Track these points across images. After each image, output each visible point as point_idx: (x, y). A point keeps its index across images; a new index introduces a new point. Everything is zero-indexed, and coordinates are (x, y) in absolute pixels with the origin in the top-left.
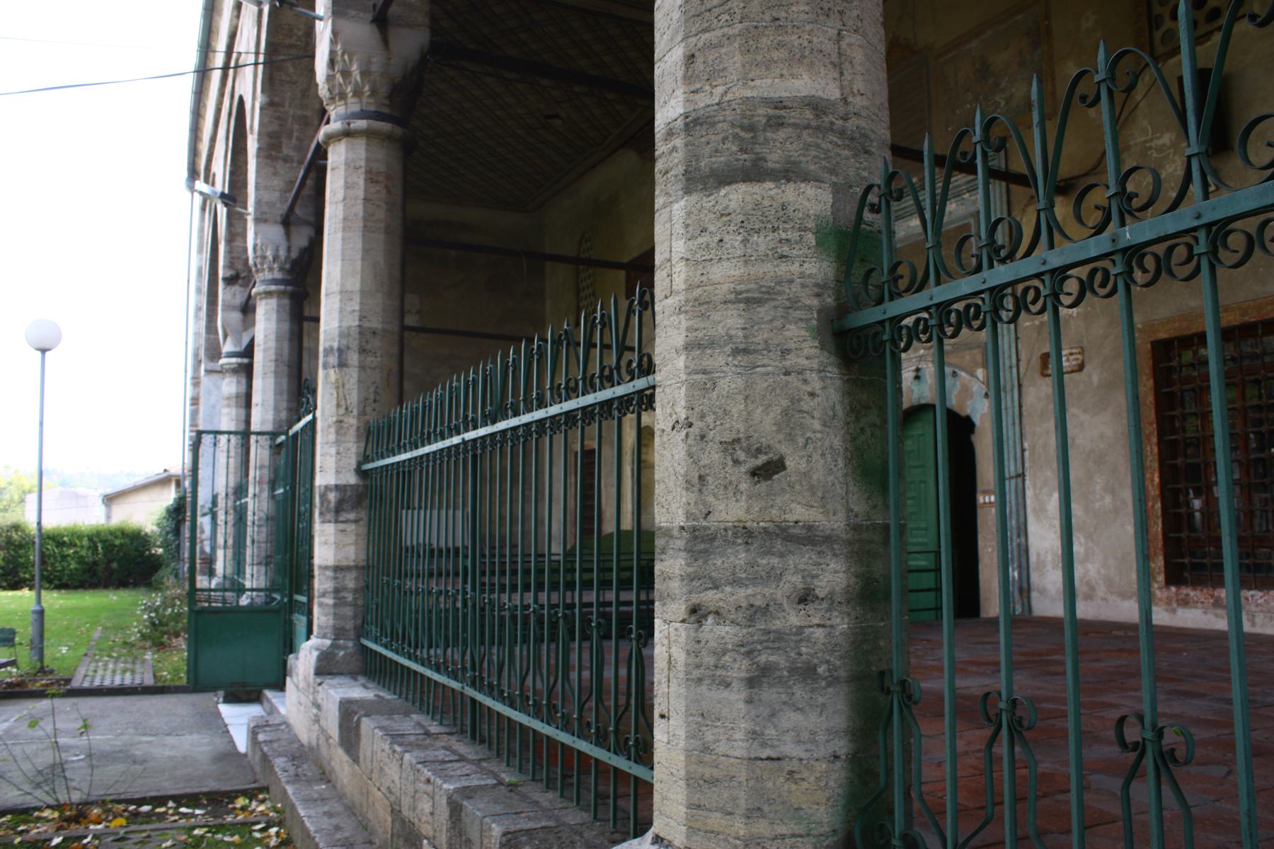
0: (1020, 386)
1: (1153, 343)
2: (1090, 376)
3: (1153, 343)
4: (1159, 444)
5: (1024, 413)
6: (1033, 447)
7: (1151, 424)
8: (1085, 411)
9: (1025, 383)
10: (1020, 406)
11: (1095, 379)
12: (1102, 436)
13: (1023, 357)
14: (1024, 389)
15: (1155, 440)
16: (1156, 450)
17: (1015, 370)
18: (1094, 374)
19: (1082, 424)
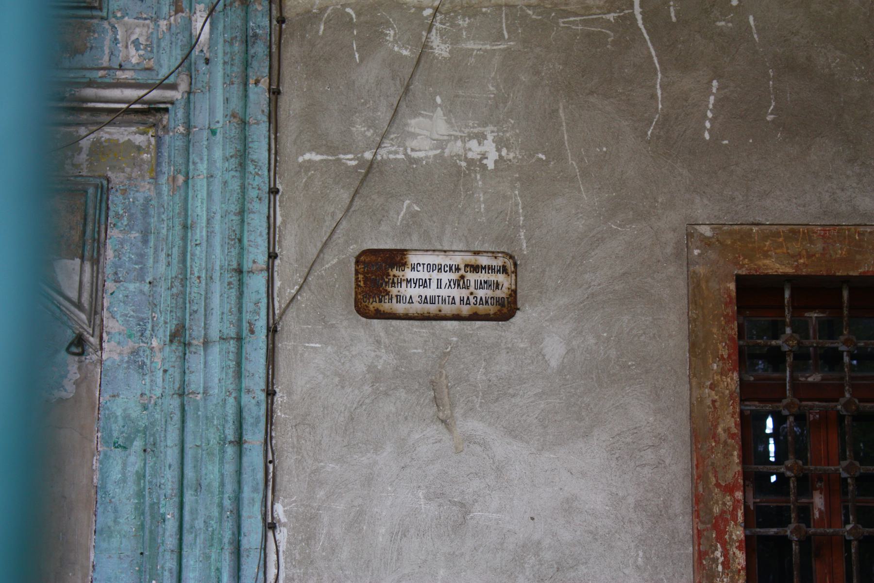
0: (272, 331)
1: (740, 280)
2: (536, 339)
3: (740, 280)
4: (750, 545)
5: (279, 414)
6: (307, 524)
7: (729, 489)
8: (512, 433)
9: (290, 325)
10: (270, 393)
11: (555, 349)
12: (569, 507)
13: (288, 248)
14: (284, 345)
15: (738, 533)
16: (740, 559)
17: (257, 283)
18: (548, 334)
19: (499, 470)
